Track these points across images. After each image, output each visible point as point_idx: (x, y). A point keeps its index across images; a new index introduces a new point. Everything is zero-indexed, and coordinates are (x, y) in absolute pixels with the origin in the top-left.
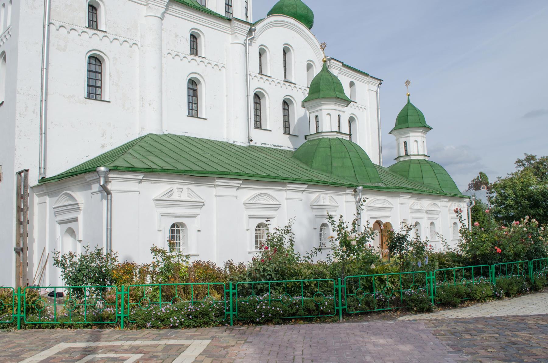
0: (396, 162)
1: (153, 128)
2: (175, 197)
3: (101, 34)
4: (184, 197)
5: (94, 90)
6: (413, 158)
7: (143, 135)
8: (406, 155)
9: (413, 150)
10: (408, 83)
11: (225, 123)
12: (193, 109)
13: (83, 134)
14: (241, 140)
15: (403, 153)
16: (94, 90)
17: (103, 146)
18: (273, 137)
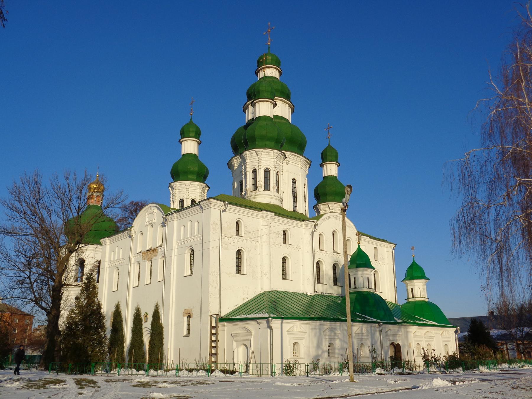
0: (406, 301)
1: (267, 289)
2: (295, 329)
3: (242, 238)
4: (299, 329)
5: (239, 269)
6: (417, 299)
7: (262, 292)
8: (413, 297)
9: (417, 294)
10: (413, 248)
11: (302, 283)
12: (284, 276)
13: (236, 293)
14: (310, 292)
15: (411, 296)
16: (239, 269)
17: (244, 299)
18: (328, 288)
